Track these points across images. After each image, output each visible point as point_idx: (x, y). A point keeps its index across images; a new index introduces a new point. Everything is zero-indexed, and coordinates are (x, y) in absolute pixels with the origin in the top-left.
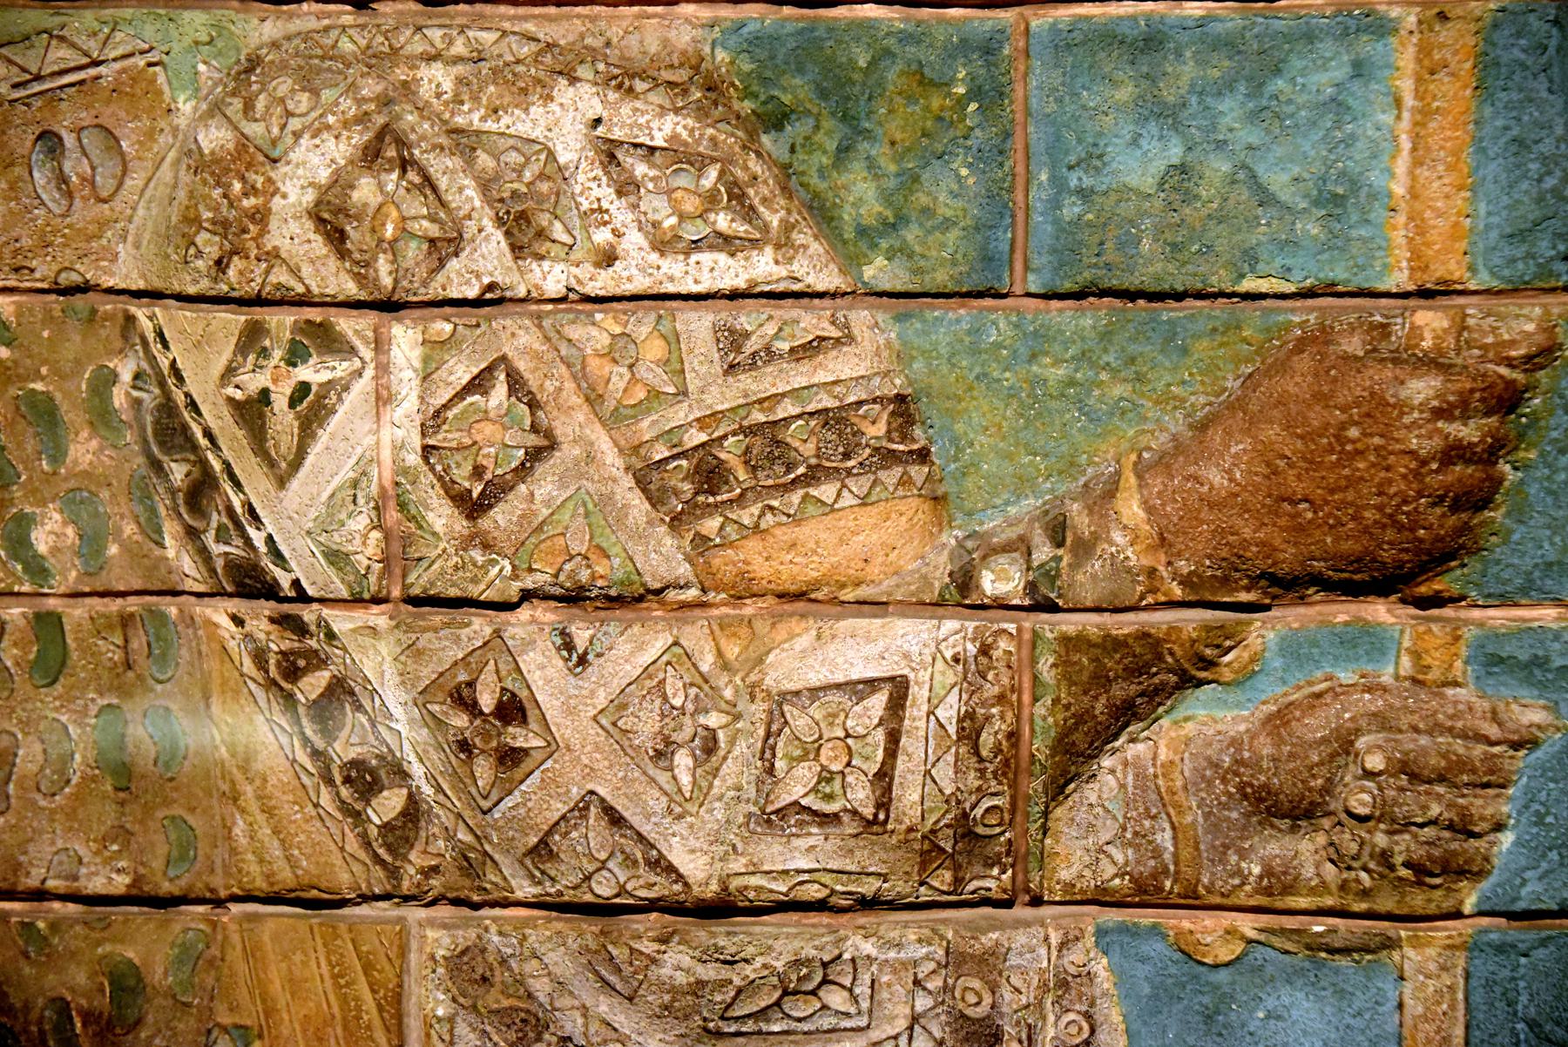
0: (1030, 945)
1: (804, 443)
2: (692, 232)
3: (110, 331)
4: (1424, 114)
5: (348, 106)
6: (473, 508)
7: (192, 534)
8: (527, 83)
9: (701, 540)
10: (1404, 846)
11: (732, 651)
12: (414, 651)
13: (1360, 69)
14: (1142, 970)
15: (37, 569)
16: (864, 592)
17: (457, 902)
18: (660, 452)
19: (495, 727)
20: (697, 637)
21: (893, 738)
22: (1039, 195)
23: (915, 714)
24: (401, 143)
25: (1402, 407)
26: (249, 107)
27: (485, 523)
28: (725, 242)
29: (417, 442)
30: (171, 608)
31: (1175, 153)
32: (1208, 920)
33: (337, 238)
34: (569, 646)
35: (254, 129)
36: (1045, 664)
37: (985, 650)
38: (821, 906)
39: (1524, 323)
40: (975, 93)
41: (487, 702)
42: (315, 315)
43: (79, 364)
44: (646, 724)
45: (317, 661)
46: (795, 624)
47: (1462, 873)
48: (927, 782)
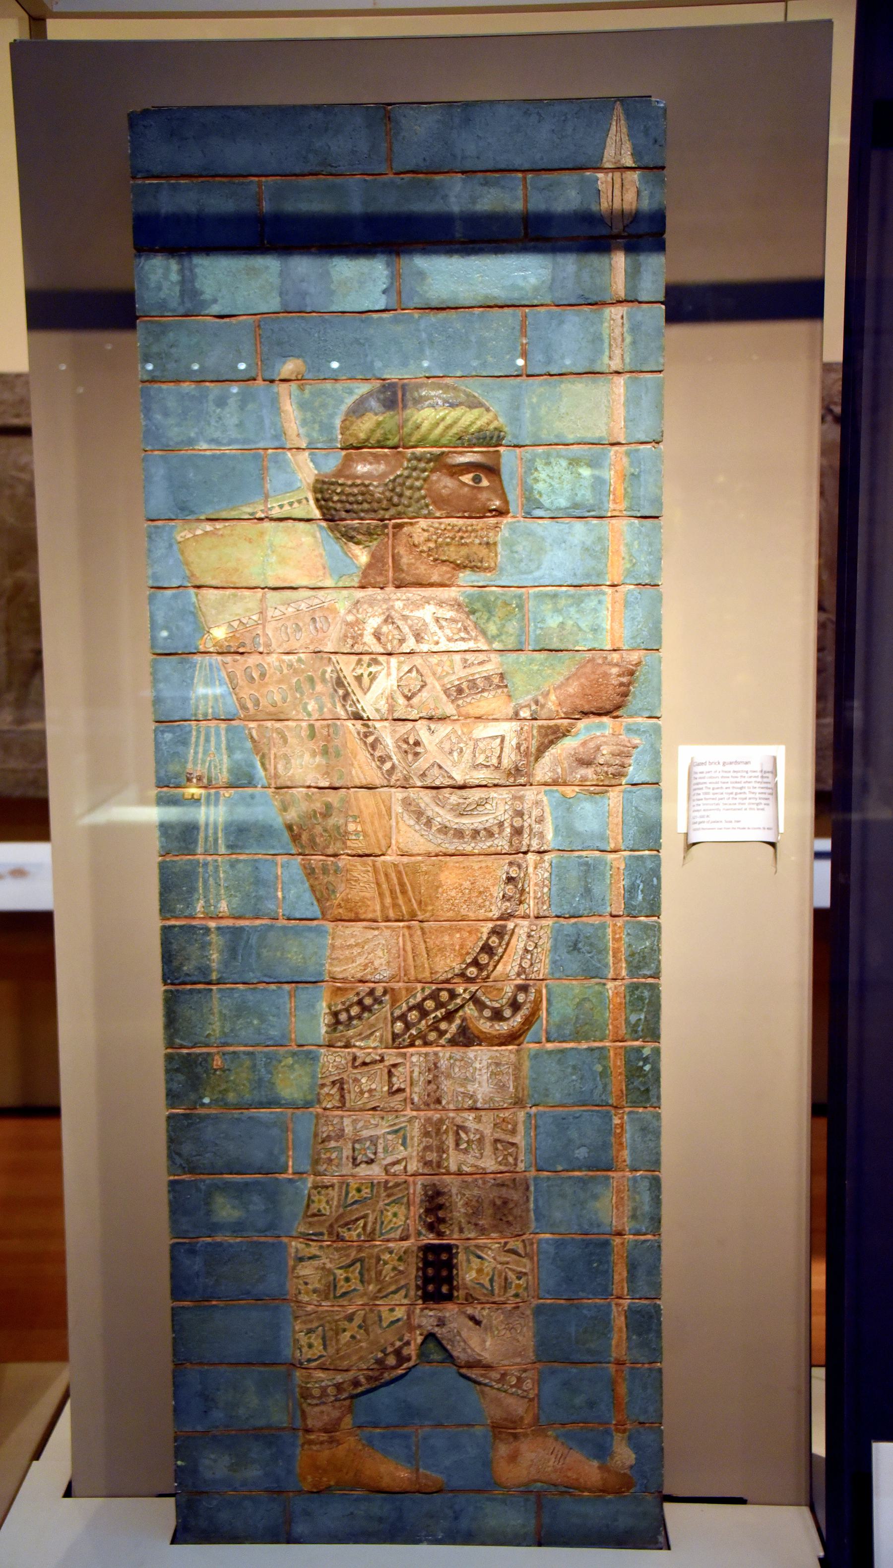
0: (530, 794)
1: (481, 684)
2: (456, 637)
3: (326, 661)
4: (613, 612)
5: (380, 611)
6: (409, 699)
7: (344, 706)
8: (417, 606)
9: (458, 706)
10: (611, 770)
11: (465, 730)
12: (394, 731)
13: (600, 602)
14: (554, 800)
15: (309, 714)
16: (494, 717)
17: (403, 787)
18: (449, 686)
19: (413, 748)
20: (457, 727)
21: (502, 749)
22: (531, 629)
23: (506, 743)
24: (392, 618)
25: (611, 674)
26: (358, 611)
27: (411, 702)
28: (463, 639)
29: (396, 684)
30: (338, 722)
31: (561, 619)
32: (568, 788)
33: (379, 639)
34: (430, 729)
35: (360, 616)
36: (535, 732)
37: (522, 729)
38: (485, 786)
39: (635, 657)
40: (517, 606)
41: (411, 742)
42: (373, 656)
43: (319, 668)
44: (447, 746)
45: (371, 734)
46: (479, 724)
47: (622, 775)
48: (509, 758)
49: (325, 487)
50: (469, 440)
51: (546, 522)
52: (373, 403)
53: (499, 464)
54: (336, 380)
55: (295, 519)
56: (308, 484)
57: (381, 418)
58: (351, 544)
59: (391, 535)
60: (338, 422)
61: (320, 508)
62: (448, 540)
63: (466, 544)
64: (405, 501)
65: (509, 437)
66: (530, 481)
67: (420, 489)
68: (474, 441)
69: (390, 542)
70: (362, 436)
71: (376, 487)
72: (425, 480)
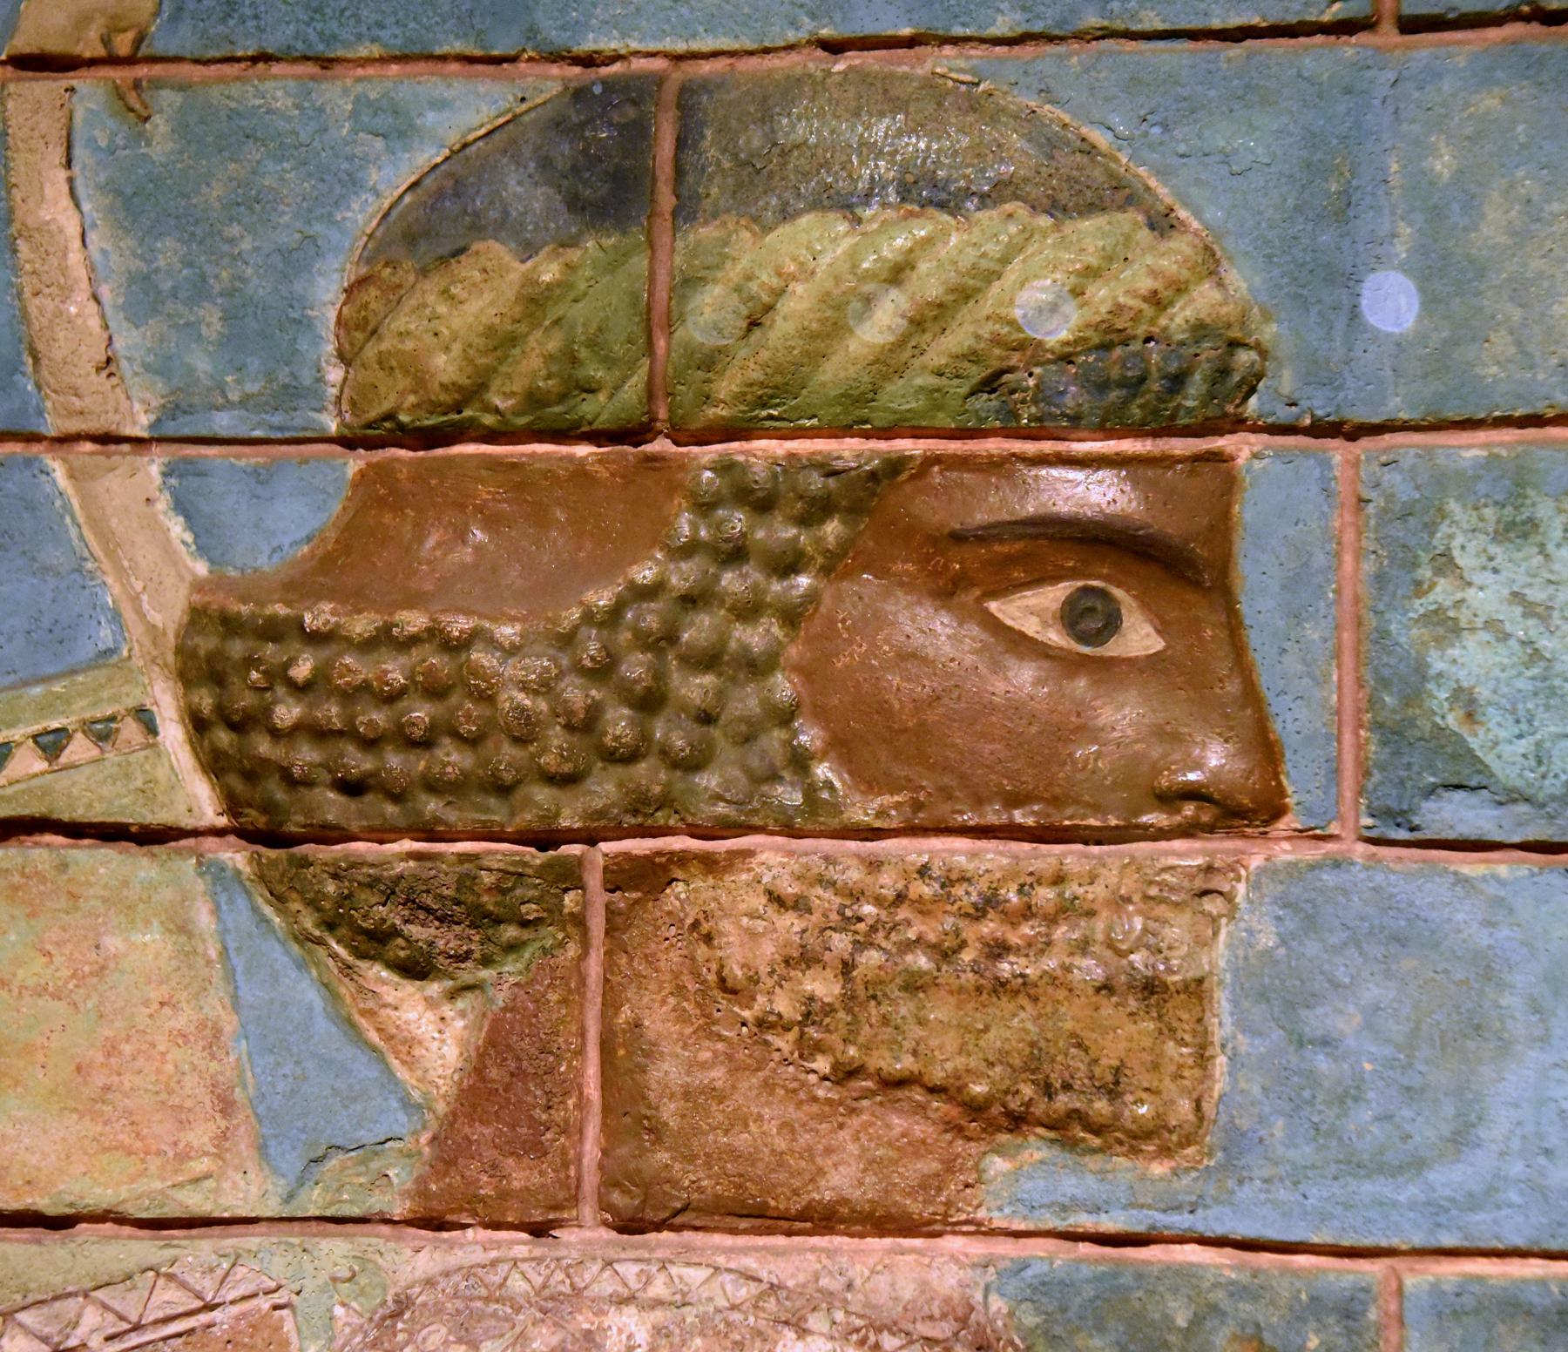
49: (237, 648)
50: (1041, 394)
51: (1502, 867)
52: (522, 192)
53: (1221, 528)
54: (326, 63)
55: (76, 831)
56: (154, 633)
57: (549, 273)
58: (376, 973)
59: (597, 924)
60: (326, 294)
61: (214, 765)
62: (922, 961)
63: (1021, 988)
64: (672, 733)
65: (1285, 380)
66: (1405, 630)
67: (757, 667)
68: (1073, 397)
69: (594, 967)
70: (445, 367)
71: (513, 651)
72: (792, 617)
